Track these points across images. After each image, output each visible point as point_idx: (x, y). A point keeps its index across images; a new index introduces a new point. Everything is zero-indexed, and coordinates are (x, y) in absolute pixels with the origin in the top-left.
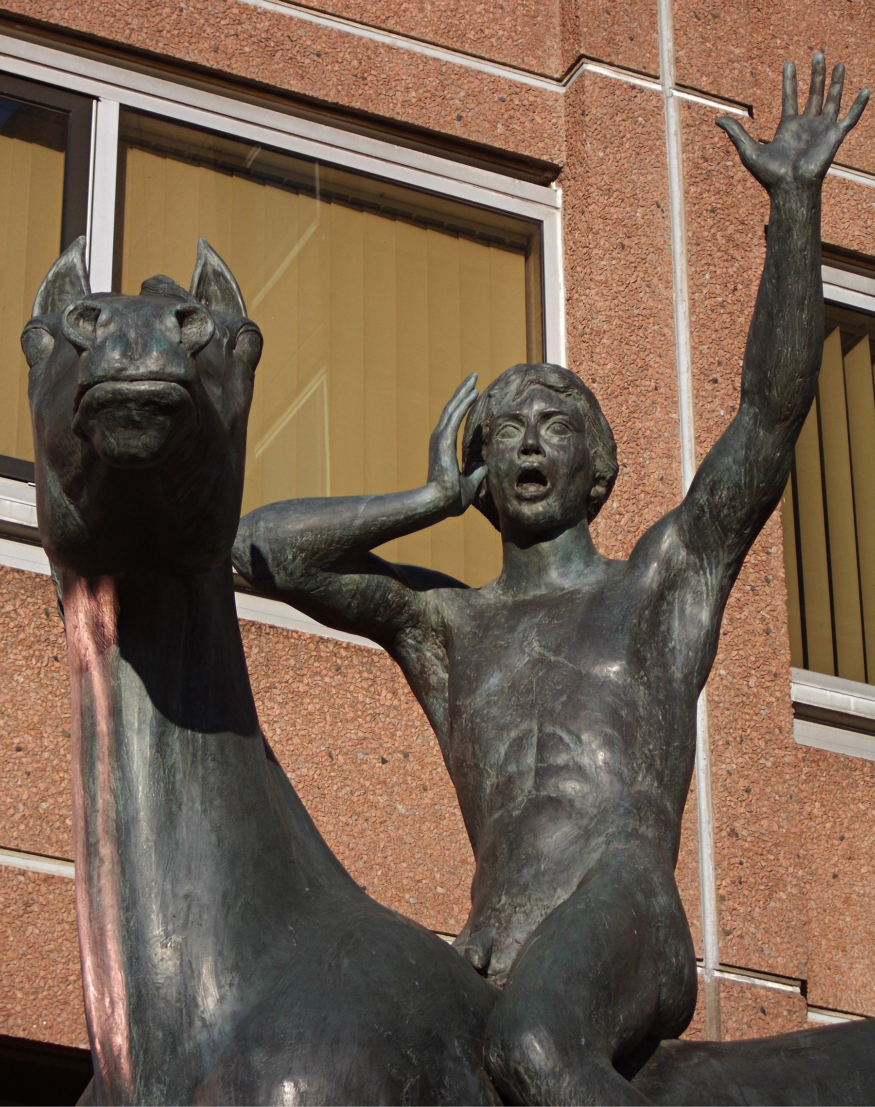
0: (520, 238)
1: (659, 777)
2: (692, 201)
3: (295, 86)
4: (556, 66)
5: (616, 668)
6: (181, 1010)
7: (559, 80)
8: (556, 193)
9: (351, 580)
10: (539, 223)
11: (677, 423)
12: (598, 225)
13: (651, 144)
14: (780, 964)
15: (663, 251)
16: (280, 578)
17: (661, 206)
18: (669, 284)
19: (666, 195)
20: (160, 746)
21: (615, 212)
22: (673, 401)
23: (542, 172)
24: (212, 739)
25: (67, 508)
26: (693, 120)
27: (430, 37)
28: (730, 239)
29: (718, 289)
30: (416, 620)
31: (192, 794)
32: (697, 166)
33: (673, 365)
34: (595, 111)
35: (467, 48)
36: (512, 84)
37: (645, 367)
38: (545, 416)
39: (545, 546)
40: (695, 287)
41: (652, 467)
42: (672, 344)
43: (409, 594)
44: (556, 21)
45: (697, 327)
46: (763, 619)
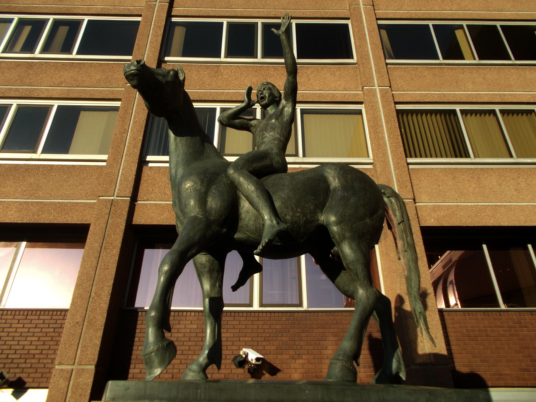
0: (360, 112)
1: (280, 135)
2: (382, 101)
3: (324, 101)
4: (361, 89)
5: (273, 121)
8: (363, 105)
9: (237, 121)
10: (361, 110)
13: (375, 95)
14: (409, 197)
15: (379, 108)
16: (225, 123)
17: (377, 102)
18: (380, 112)
20: (175, 139)
23: (361, 103)
24: (185, 138)
26: (381, 90)
30: (251, 126)
31: (180, 145)
33: (382, 122)
38: (264, 89)
39: (268, 108)
40: (384, 111)
43: (249, 122)
45: (385, 116)
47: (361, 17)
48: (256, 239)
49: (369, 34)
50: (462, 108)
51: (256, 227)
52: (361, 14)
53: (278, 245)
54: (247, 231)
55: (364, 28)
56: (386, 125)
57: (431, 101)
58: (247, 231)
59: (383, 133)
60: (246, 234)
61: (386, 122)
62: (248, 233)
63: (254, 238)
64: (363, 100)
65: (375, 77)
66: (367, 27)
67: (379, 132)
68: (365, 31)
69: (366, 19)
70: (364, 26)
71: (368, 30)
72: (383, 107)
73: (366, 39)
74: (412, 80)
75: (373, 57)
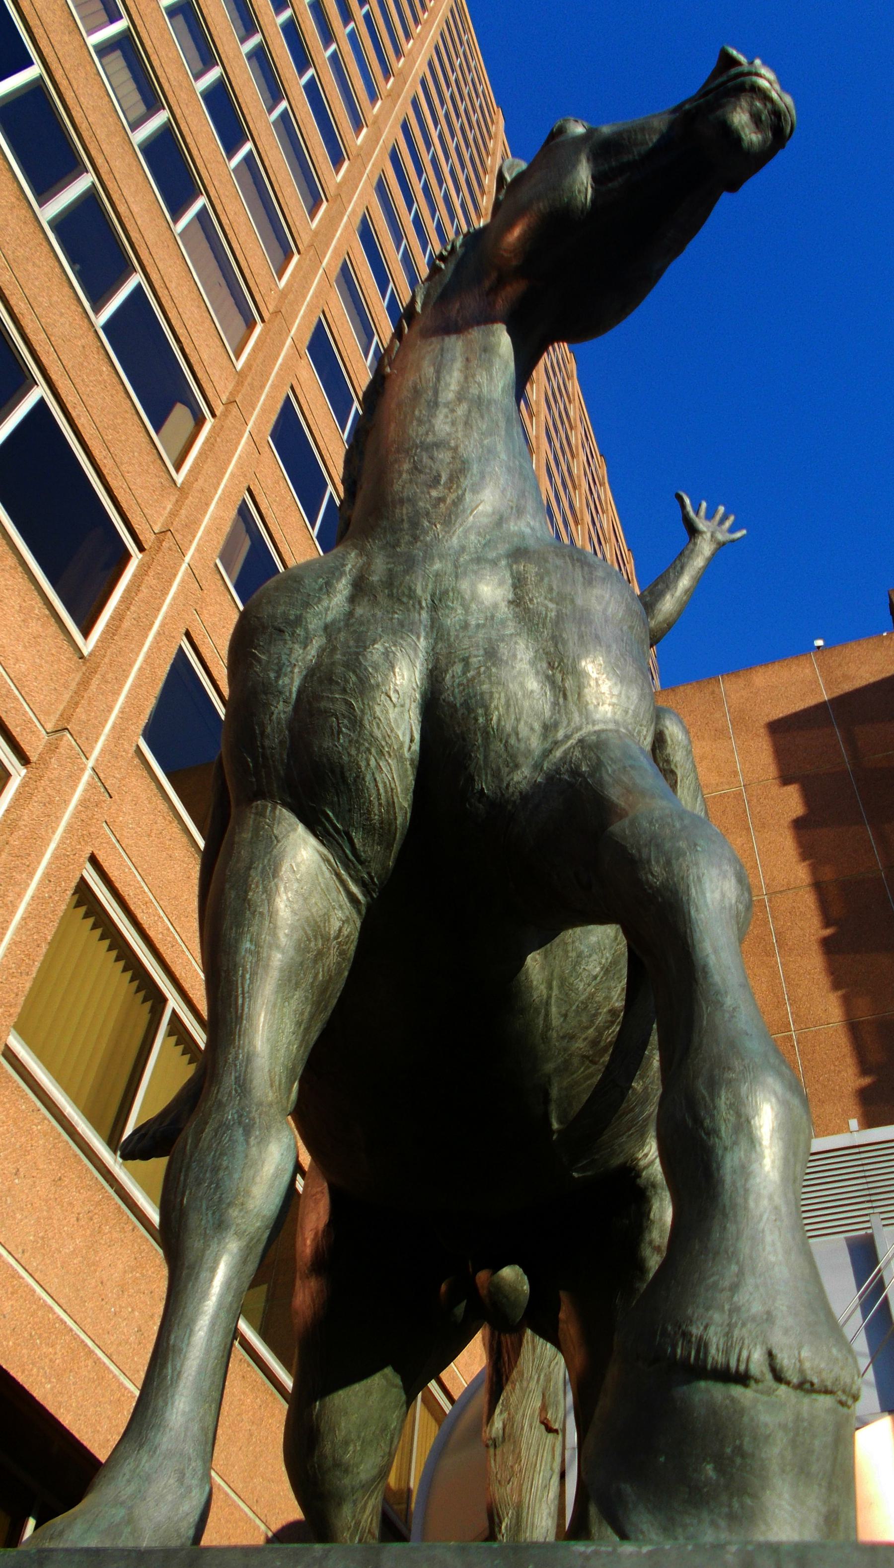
4: (50, 727)
6: (512, 508)
7: (48, 733)
11: (28, 885)
12: (41, 789)
17: (66, 802)
18: (54, 832)
19: (70, 801)
21: (49, 791)
22: (31, 875)
25: (586, 189)
27: (12, 676)
28: (83, 835)
29: (69, 849)
32: (85, 800)
33: (39, 863)
34: (62, 750)
35: (23, 692)
36: (31, 719)
37: (29, 855)
40: (62, 841)
41: (11, 894)
42: (43, 855)
44: (59, 713)
45: (55, 857)
46: (18, 988)
47: (170, 582)
48: (545, 1039)
49: (159, 633)
50: (178, 1010)
51: (592, 996)
52: (175, 575)
53: (550, 1125)
54: (563, 981)
55: (159, 610)
56: (41, 882)
57: (145, 926)
58: (563, 981)
59: (20, 896)
60: (550, 987)
61: (47, 876)
62: (555, 992)
63: (548, 1027)
64: (33, 759)
65: (102, 738)
66: (165, 618)
67: (17, 884)
68: (156, 617)
69: (174, 599)
70: (161, 604)
71: (163, 625)
72: (70, 829)
73: (147, 636)
74: (149, 836)
75: (129, 692)
